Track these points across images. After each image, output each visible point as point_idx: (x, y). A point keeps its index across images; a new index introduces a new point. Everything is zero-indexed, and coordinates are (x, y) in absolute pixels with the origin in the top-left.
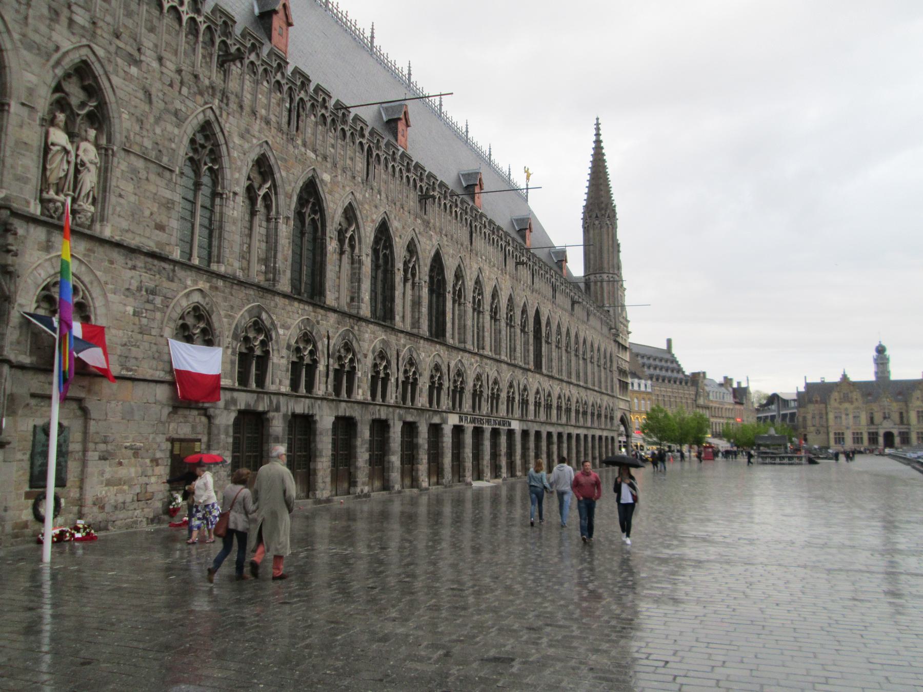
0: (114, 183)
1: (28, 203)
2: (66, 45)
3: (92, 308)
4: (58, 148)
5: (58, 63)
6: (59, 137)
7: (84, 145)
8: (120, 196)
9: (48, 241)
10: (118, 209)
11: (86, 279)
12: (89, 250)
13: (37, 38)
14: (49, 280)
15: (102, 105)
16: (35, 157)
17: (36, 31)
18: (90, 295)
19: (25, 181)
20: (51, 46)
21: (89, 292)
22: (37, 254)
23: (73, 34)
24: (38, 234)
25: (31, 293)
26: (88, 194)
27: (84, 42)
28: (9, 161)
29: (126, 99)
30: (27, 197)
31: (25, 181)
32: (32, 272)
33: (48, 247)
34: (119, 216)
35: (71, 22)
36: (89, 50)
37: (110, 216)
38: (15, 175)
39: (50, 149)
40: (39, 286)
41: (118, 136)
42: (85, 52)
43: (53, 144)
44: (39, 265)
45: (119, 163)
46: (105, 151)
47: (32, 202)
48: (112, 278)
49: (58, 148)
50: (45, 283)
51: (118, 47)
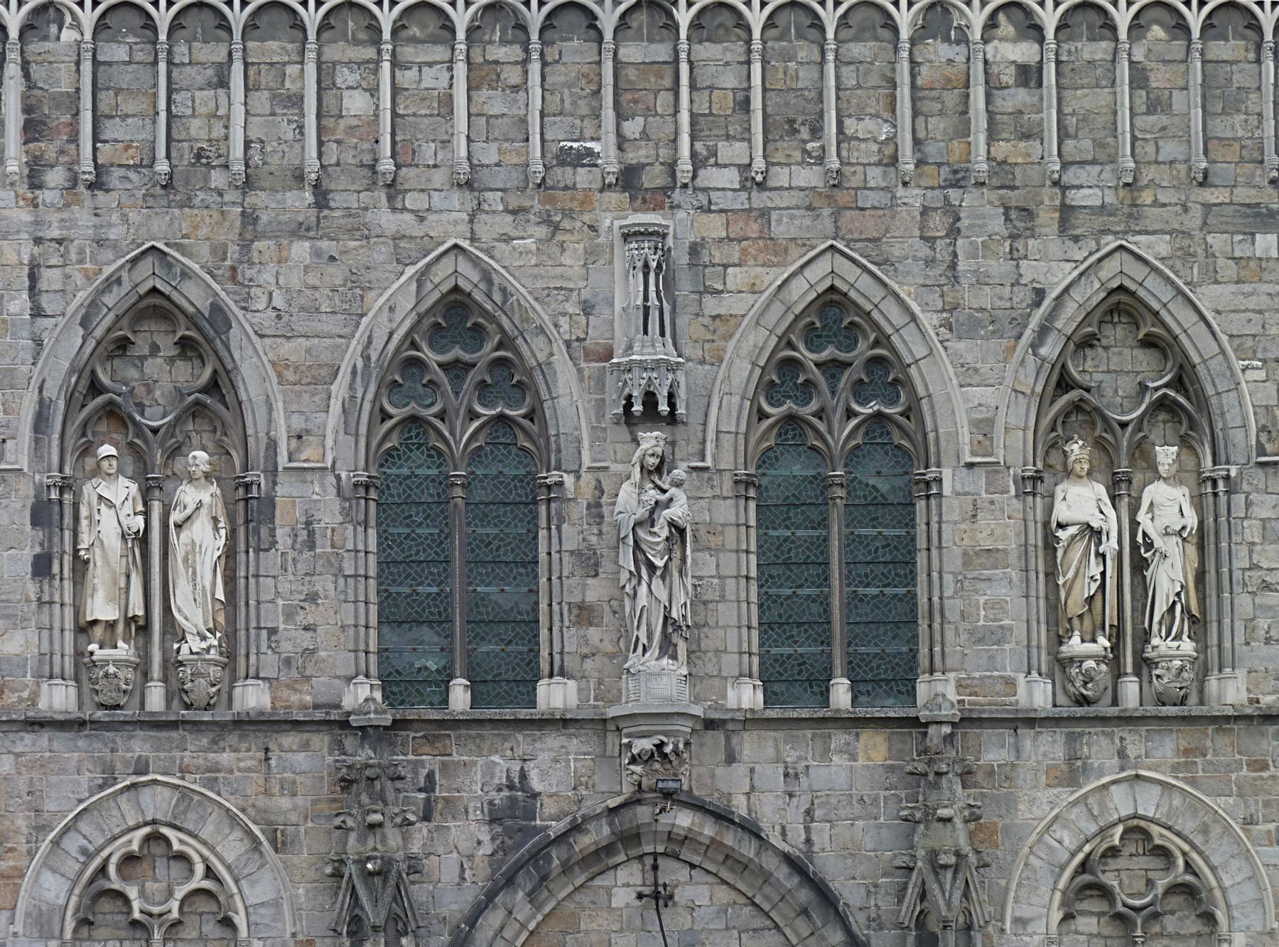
0: (1241, 561)
1: (1011, 683)
2: (1063, 275)
3: (1217, 893)
4: (1072, 530)
5: (1043, 331)
6: (1082, 501)
7: (1156, 492)
8: (1267, 587)
9: (1072, 758)
10: (1263, 623)
11: (1188, 825)
12: (1187, 752)
13: (986, 298)
14: (1087, 848)
15: (1184, 378)
16: (1015, 574)
17: (981, 281)
18: (1206, 860)
19: (999, 635)
20: (1023, 296)
21: (1200, 853)
22: (1045, 795)
23: (1076, 239)
24: (1047, 748)
25: (1045, 890)
26: (1172, 609)
27: (1110, 243)
28: (954, 607)
29: (1256, 329)
30: (1009, 673)
31: (999, 635)
32: (1039, 840)
33: (1073, 771)
34: (1268, 641)
35: (1066, 211)
36: (1125, 256)
37: (1241, 650)
38: (971, 633)
39: (1058, 539)
40: (1063, 868)
41: (1237, 436)
42: (1109, 270)
43: (1061, 526)
44: (1056, 817)
45: (1248, 504)
46: (1210, 491)
47: (1021, 678)
48: (1267, 804)
49: (1072, 530)
50: (1080, 856)
51: (1207, 207)
